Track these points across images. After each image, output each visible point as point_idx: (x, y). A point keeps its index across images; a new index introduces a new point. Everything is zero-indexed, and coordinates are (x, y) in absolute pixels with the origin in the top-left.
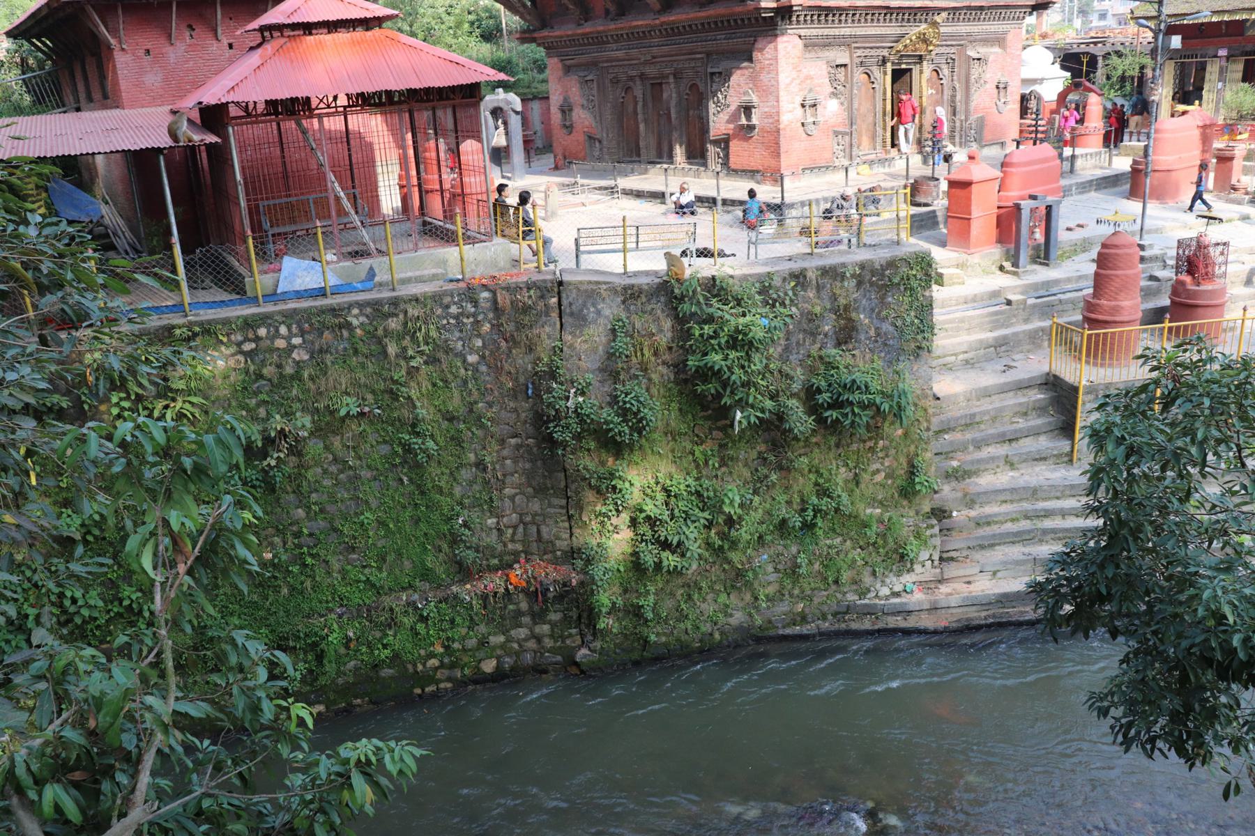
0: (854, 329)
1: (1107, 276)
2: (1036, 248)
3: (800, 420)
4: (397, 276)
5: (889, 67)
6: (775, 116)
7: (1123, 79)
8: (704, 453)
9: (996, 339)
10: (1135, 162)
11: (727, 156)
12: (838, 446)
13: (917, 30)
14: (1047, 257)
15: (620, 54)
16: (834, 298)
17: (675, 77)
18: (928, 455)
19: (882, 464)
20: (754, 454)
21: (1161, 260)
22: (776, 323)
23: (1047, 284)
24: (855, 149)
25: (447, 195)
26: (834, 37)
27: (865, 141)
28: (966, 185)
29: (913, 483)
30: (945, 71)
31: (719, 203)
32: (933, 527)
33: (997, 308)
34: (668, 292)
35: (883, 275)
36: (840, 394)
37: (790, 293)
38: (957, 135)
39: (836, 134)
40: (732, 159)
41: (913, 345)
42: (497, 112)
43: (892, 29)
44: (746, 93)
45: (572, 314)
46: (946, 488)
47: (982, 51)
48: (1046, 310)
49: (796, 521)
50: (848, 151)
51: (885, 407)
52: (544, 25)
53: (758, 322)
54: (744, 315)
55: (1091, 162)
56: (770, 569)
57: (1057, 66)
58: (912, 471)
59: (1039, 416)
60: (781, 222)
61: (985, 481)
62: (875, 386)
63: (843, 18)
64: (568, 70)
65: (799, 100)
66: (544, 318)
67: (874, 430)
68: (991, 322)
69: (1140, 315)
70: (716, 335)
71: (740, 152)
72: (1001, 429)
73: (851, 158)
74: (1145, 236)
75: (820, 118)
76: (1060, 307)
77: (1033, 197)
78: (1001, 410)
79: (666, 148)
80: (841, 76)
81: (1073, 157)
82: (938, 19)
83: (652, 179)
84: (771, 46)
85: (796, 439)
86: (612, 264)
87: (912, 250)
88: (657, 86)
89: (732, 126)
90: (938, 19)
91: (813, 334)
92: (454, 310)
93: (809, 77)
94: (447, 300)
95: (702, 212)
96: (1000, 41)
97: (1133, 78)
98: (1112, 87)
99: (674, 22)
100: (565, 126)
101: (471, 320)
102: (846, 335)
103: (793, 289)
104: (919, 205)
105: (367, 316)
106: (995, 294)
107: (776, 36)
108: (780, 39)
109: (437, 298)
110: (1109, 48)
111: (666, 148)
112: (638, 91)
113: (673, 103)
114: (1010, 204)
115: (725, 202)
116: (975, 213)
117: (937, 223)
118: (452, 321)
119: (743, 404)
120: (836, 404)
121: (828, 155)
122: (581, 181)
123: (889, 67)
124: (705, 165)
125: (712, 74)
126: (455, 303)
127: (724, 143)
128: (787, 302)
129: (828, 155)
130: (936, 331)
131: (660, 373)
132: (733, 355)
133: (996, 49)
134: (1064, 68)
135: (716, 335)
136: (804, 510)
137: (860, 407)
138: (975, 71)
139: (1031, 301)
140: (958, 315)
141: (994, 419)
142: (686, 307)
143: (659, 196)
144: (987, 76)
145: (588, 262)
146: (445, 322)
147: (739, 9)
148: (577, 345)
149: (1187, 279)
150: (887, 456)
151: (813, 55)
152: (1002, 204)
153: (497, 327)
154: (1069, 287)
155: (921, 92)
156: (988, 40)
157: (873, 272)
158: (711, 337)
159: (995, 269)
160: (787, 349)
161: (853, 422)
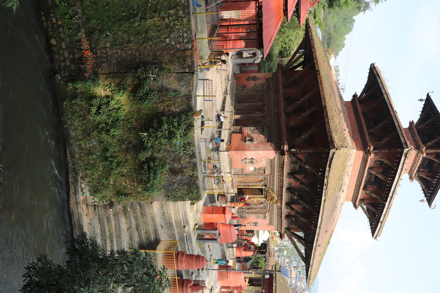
0: (175, 174)
1: (193, 259)
2: (203, 236)
3: (143, 156)
4: (198, 15)
5: (264, 187)
6: (249, 149)
7: (258, 262)
8: (132, 122)
9: (172, 223)
10: (230, 267)
11: (236, 133)
12: (135, 169)
13: (275, 197)
14: (200, 239)
15: (272, 97)
16: (186, 168)
17: (263, 116)
18: (132, 200)
19: (128, 184)
20: (132, 140)
21: (198, 276)
22: (178, 148)
23: (191, 239)
24: (237, 176)
25: (226, 35)
26: (274, 169)
27: (240, 179)
28: (224, 212)
29: (122, 195)
30: (262, 206)
31: (220, 130)
32: (107, 202)
33: (182, 223)
34: (189, 111)
35: (194, 184)
36: (153, 169)
37: (188, 153)
38: (241, 210)
39: (242, 170)
40: (235, 135)
41: (170, 194)
42: (254, 54)
43: (276, 188)
44: (257, 139)
45: (182, 77)
47: (268, 217)
48: (182, 239)
49: (108, 155)
50: (237, 173)
51: (148, 185)
52: (283, 72)
53: (178, 141)
54: (180, 137)
55: (231, 253)
56: (91, 145)
57: (263, 242)
58: (126, 195)
59: (146, 238)
61: (123, 220)
62: (156, 182)
63: (280, 172)
64: (268, 80)
65: (254, 157)
66: (181, 67)
67: (140, 182)
68: (178, 222)
69: (180, 269)
70: (174, 127)
71: (237, 137)
72: (141, 225)
73: (234, 175)
74: (206, 270)
75: (247, 164)
76: (183, 244)
77: (219, 234)
78: (148, 225)
79: (240, 112)
81: (233, 247)
82: (278, 203)
83: (229, 107)
84: (272, 149)
85: (137, 154)
86: (200, 92)
87: (202, 194)
88: (260, 110)
89: (246, 135)
90: (278, 203)
91: (174, 160)
92: (185, 35)
93: (261, 161)
94: (189, 33)
96: (271, 223)
97: (258, 265)
98: (255, 259)
99: (281, 116)
100: (249, 78)
101: (181, 41)
102: (173, 172)
103: (189, 154)
104: (218, 197)
105: (184, 3)
106: (187, 222)
107: (275, 150)
108: (274, 151)
109: (189, 29)
110: (267, 258)
111: (240, 112)
112: (259, 103)
113: (255, 115)
114: (217, 227)
115: (220, 131)
116: (215, 216)
117: (212, 203)
118: (181, 34)
119: (149, 136)
120: (149, 168)
121: (235, 167)
122: (230, 82)
123: (264, 187)
124: (233, 125)
125: (264, 129)
126: (187, 35)
127: (241, 132)
128: (185, 152)
129: (235, 167)
130: (174, 202)
131: (161, 107)
132: (167, 132)
133: (268, 222)
134: (262, 244)
135: (174, 127)
136: (112, 157)
137: (148, 176)
138: (261, 215)
139: (185, 234)
140: (180, 210)
141: (144, 222)
142: (184, 117)
143: (223, 109)
144: (260, 220)
145: (200, 83)
146: (181, 31)
147: (284, 138)
148: (171, 78)
149: (192, 284)
150: (131, 186)
151: (269, 162)
152: (217, 224)
153: (178, 50)
154: (190, 247)
155: (255, 198)
156: (271, 219)
157: (194, 181)
158: (173, 125)
159: (196, 222)
160: (169, 151)
161: (143, 174)
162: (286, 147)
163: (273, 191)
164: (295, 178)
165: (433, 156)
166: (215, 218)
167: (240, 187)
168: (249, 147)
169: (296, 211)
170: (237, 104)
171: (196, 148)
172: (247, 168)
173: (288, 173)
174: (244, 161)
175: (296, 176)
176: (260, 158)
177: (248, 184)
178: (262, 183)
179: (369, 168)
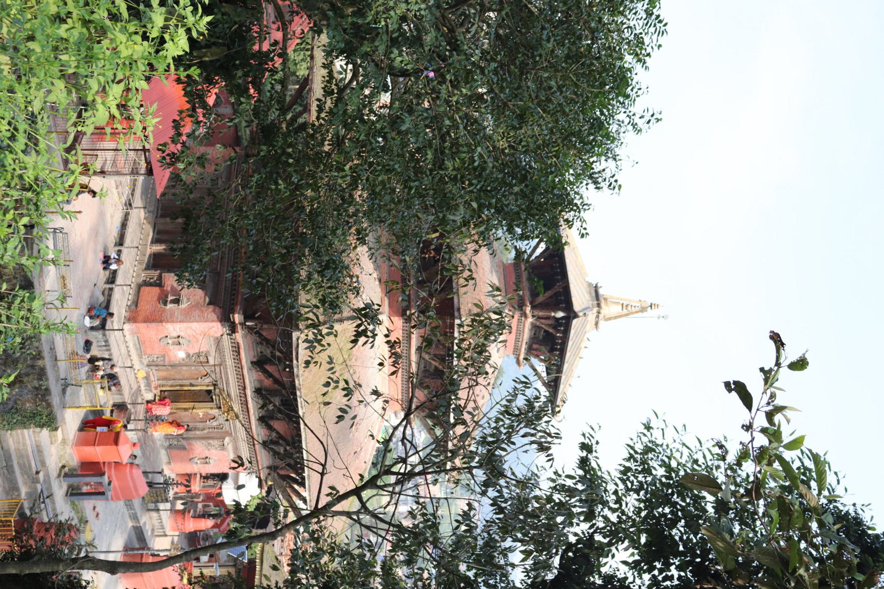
11: (151, 285)
14: (72, 495)
16: (27, 375)
24: (154, 368)
30: (215, 424)
35: (42, 401)
39: (164, 356)
43: (234, 391)
44: (188, 299)
47: (230, 447)
55: (156, 523)
60: (92, 328)
65: (182, 334)
73: (148, 366)
75: (171, 347)
77: (109, 484)
79: (164, 237)
80: (202, 359)
81: (158, 510)
89: (169, 289)
95: (103, 275)
103: (31, 354)
106: (43, 463)
107: (221, 321)
108: (219, 324)
111: (164, 237)
115: (111, 289)
121: (149, 352)
129: (149, 352)
138: (215, 443)
139: (39, 487)
140: (28, 442)
143: (120, 242)
144: (213, 451)
151: (212, 342)
152: (106, 465)
157: (43, 396)
159: (64, 462)
162: (237, 318)
163: (229, 395)
164: (265, 371)
165: (550, 322)
166: (99, 453)
167: (164, 389)
168: (172, 314)
169: (278, 433)
171: (44, 344)
172: (171, 354)
173: (252, 363)
174: (165, 341)
175: (268, 368)
176: (196, 336)
177: (180, 382)
178: (208, 380)
179: (419, 349)
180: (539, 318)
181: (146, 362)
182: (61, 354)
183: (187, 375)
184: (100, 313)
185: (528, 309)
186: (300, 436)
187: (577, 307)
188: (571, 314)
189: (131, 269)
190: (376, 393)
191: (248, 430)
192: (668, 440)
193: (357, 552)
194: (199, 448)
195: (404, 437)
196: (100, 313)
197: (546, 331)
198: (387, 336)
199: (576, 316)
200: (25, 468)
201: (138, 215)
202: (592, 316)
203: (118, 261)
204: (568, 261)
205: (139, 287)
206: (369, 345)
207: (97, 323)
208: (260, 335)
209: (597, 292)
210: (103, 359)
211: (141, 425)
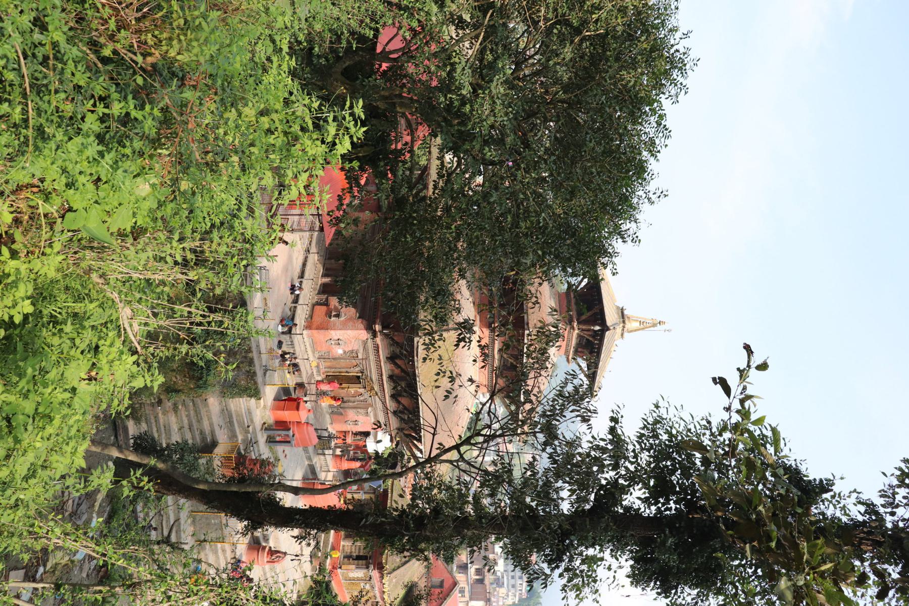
11: (321, 304)
14: (270, 442)
18: (183, 397)
27: (329, 364)
29: (172, 392)
43: (375, 377)
46: (170, 404)
47: (372, 414)
51: (201, 382)
58: (177, 391)
60: (283, 333)
62: (209, 378)
65: (341, 338)
67: (192, 378)
80: (355, 355)
95: (291, 298)
106: (252, 421)
115: (295, 307)
127: (326, 304)
139: (249, 436)
143: (302, 276)
157: (252, 377)
162: (378, 327)
165: (590, 333)
166: (287, 415)
168: (334, 325)
170: (327, 261)
174: (330, 342)
175: (398, 361)
176: (350, 339)
178: (357, 369)
179: (500, 350)
180: (583, 330)
181: (317, 356)
182: (263, 350)
183: (343, 365)
184: (288, 323)
185: (575, 324)
186: (418, 408)
187: (609, 323)
188: (605, 328)
189: (308, 294)
190: (471, 380)
191: (384, 403)
192: (671, 415)
193: (456, 487)
194: (351, 414)
195: (490, 411)
196: (288, 323)
197: (587, 339)
198: (479, 342)
199: (608, 329)
200: (241, 424)
201: (314, 258)
202: (619, 330)
203: (300, 288)
204: (603, 291)
205: (314, 305)
206: (466, 348)
207: (286, 329)
208: (393, 340)
209: (622, 313)
210: (289, 353)
211: (313, 398)
